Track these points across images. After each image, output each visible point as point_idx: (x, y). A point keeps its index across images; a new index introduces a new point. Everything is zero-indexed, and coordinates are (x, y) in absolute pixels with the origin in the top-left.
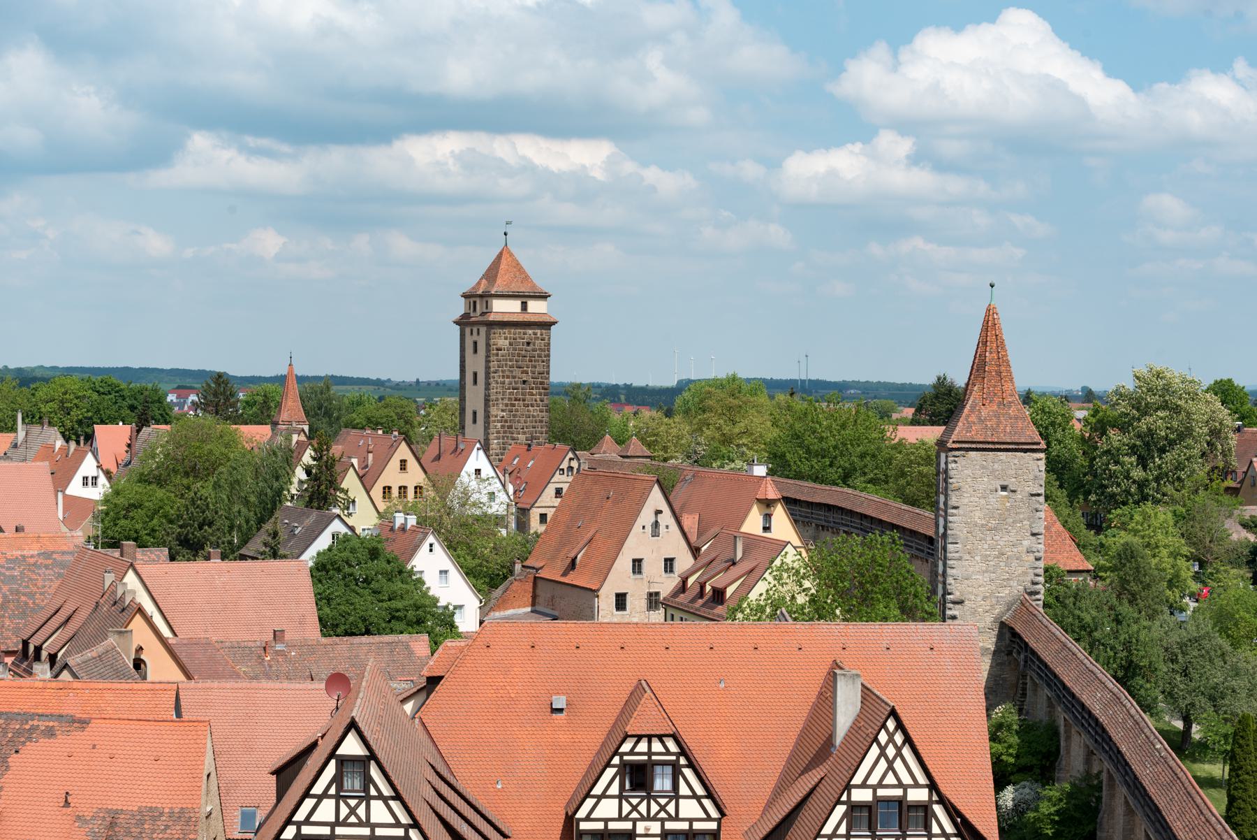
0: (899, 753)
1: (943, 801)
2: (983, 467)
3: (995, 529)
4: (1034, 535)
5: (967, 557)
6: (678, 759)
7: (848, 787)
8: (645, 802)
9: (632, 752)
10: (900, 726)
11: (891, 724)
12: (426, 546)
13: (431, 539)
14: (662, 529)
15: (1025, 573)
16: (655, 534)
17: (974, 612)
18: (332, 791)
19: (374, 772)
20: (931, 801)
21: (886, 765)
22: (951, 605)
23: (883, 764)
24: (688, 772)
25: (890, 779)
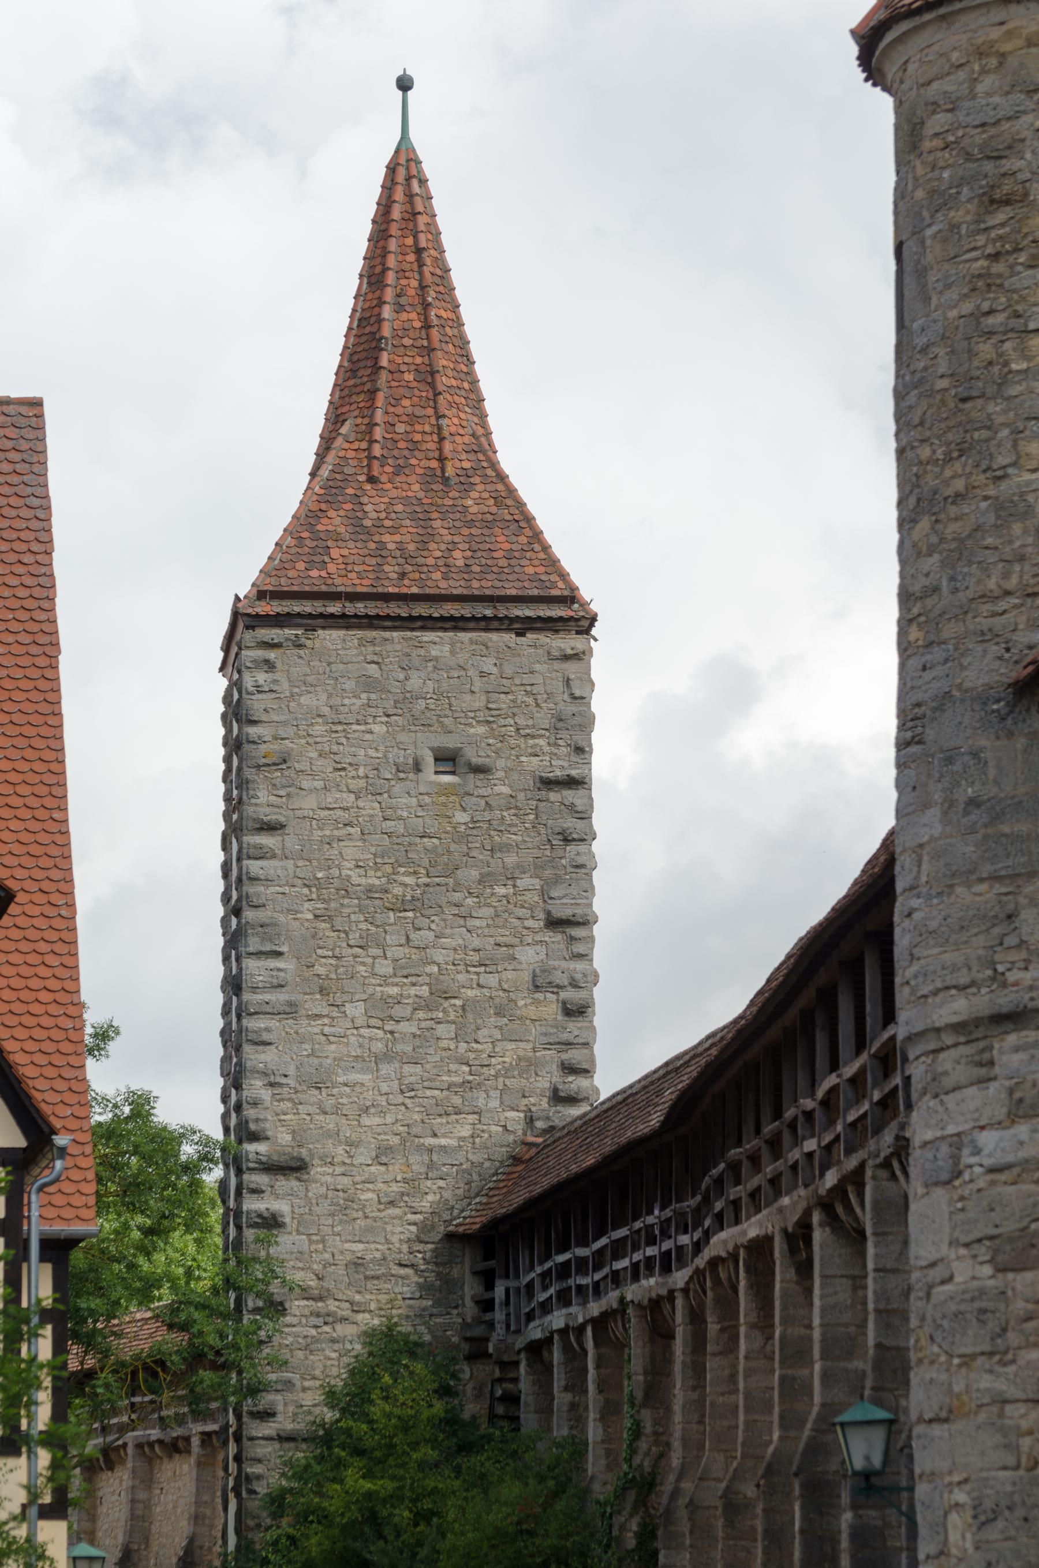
5: (316, 1005)
15: (528, 1065)
17: (346, 1205)
22: (260, 1179)
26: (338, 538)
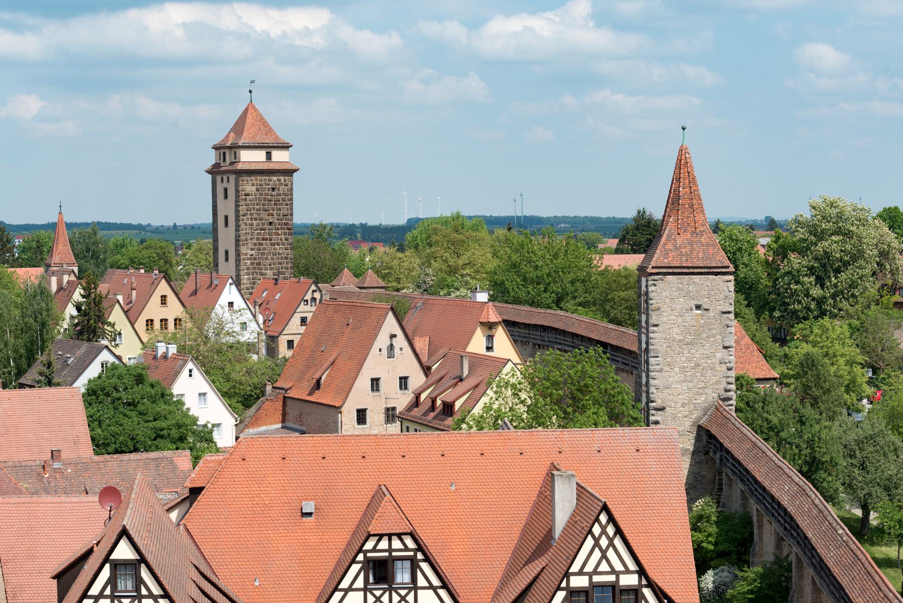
0: (611, 544)
1: (651, 585)
2: (680, 289)
3: (691, 343)
4: (725, 348)
5: (667, 368)
6: (416, 555)
7: (567, 575)
8: (387, 594)
9: (374, 550)
10: (611, 519)
11: (603, 518)
12: (186, 372)
13: (190, 365)
14: (397, 351)
15: (718, 382)
16: (391, 355)
17: (675, 417)
18: (108, 592)
19: (145, 574)
20: (640, 585)
21: (600, 555)
22: (652, 412)
23: (597, 554)
24: (425, 566)
25: (604, 567)
26: (671, 250)
